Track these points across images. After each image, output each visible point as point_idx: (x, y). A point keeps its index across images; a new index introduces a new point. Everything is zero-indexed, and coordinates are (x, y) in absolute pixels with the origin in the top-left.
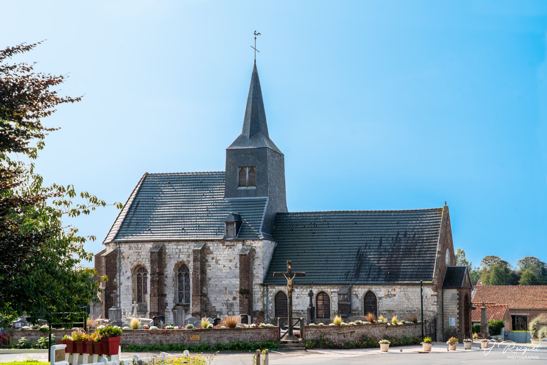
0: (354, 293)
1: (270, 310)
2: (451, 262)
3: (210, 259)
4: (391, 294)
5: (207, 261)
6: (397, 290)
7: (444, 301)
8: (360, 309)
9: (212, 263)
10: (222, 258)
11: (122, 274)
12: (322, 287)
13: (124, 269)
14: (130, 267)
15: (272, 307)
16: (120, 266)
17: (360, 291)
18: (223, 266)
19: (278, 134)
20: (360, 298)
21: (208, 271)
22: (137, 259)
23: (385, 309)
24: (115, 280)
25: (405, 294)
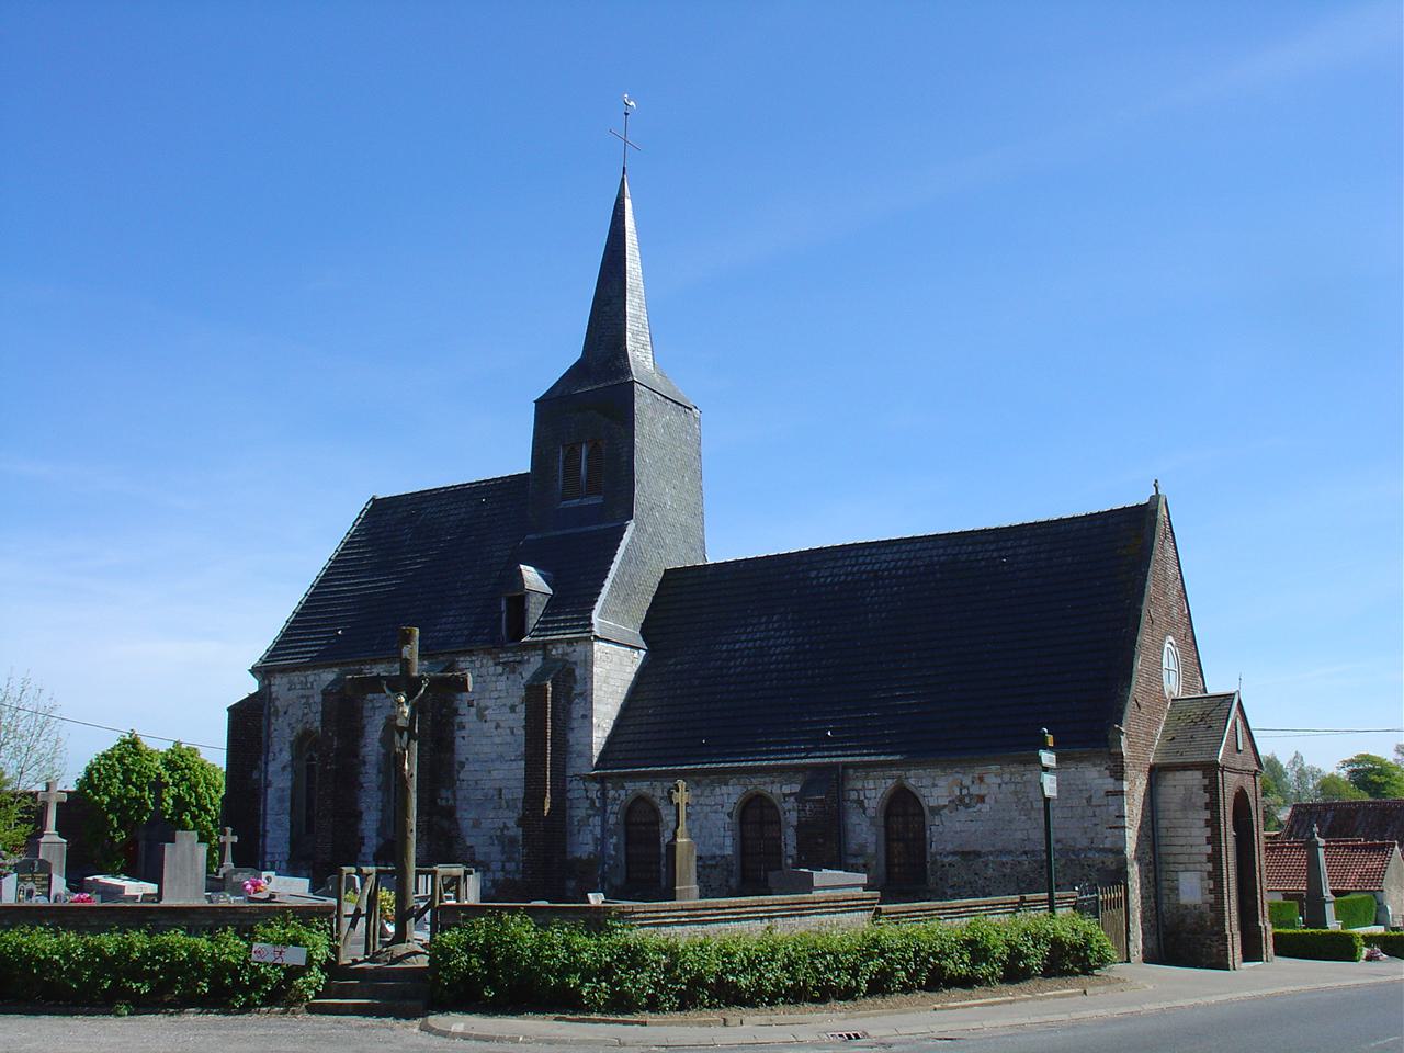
0: (853, 795)
1: (611, 857)
2: (1187, 686)
3: (463, 708)
4: (969, 795)
5: (456, 712)
6: (991, 780)
7: (1161, 815)
8: (871, 850)
9: (468, 717)
10: (490, 703)
11: (271, 756)
12: (754, 781)
13: (275, 748)
14: (289, 736)
15: (616, 847)
16: (269, 736)
17: (873, 791)
18: (494, 725)
19: (640, 353)
20: (871, 813)
21: (459, 741)
22: (304, 715)
23: (949, 848)
24: (255, 776)
25: (1015, 793)
